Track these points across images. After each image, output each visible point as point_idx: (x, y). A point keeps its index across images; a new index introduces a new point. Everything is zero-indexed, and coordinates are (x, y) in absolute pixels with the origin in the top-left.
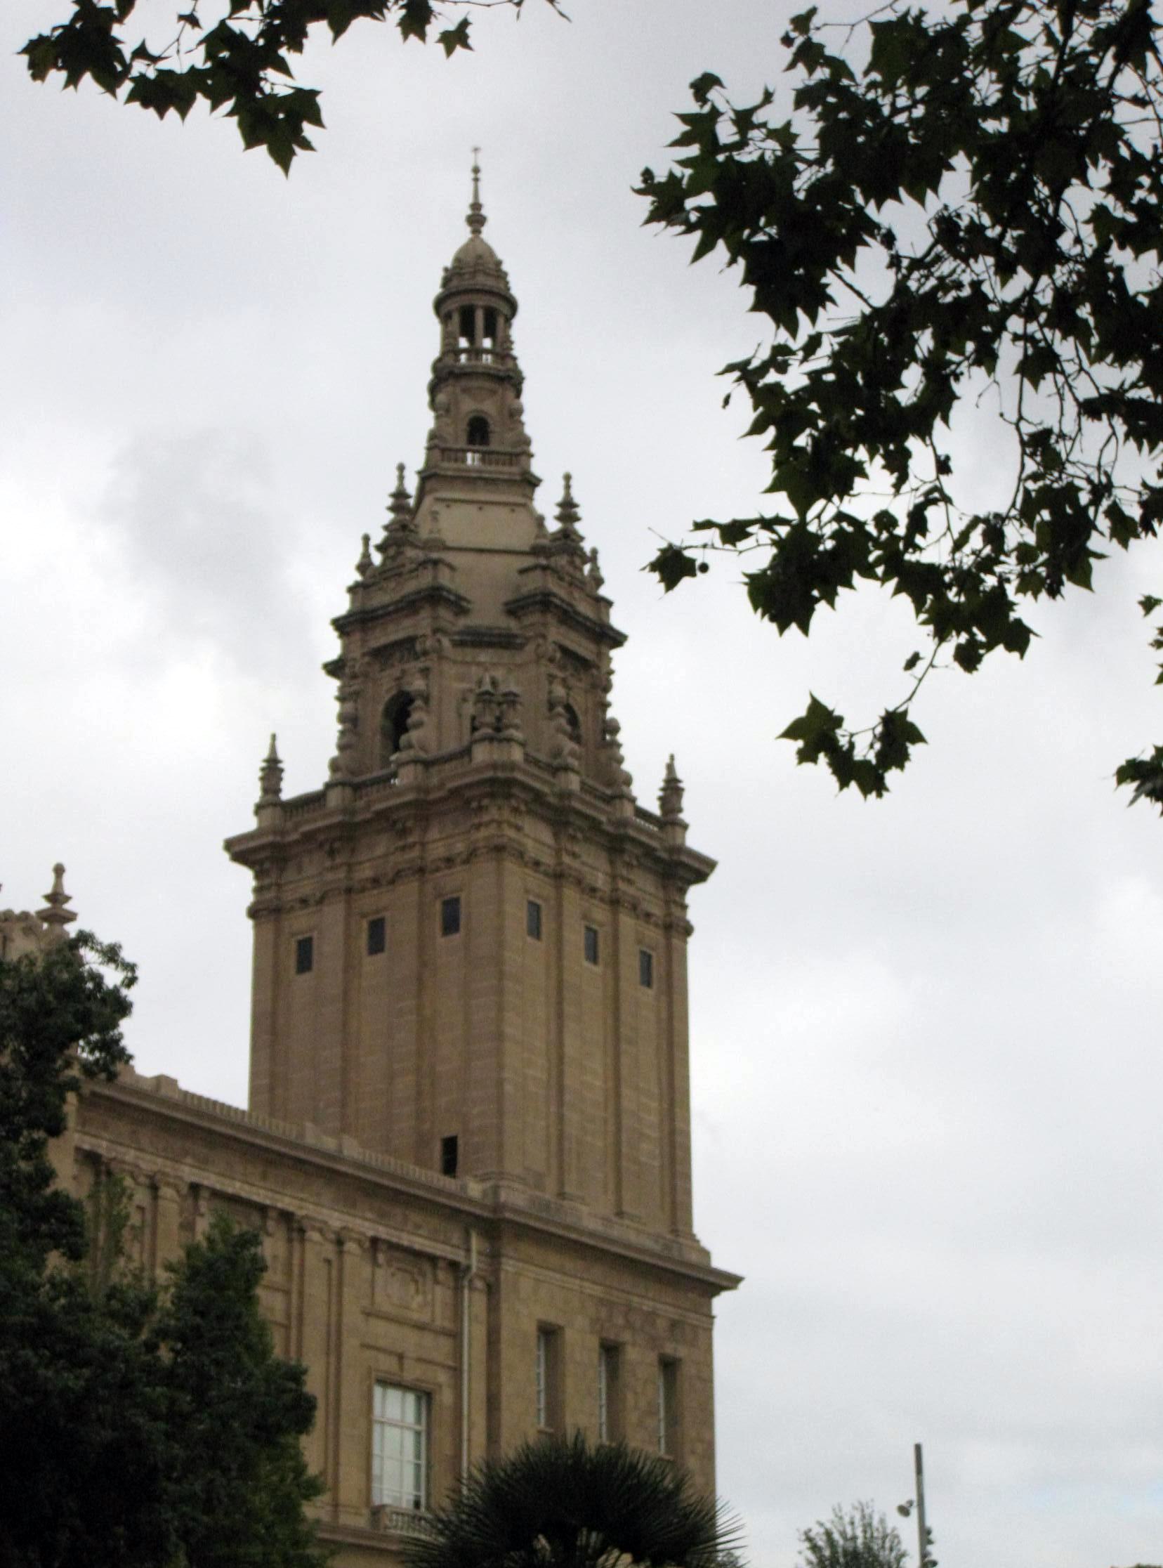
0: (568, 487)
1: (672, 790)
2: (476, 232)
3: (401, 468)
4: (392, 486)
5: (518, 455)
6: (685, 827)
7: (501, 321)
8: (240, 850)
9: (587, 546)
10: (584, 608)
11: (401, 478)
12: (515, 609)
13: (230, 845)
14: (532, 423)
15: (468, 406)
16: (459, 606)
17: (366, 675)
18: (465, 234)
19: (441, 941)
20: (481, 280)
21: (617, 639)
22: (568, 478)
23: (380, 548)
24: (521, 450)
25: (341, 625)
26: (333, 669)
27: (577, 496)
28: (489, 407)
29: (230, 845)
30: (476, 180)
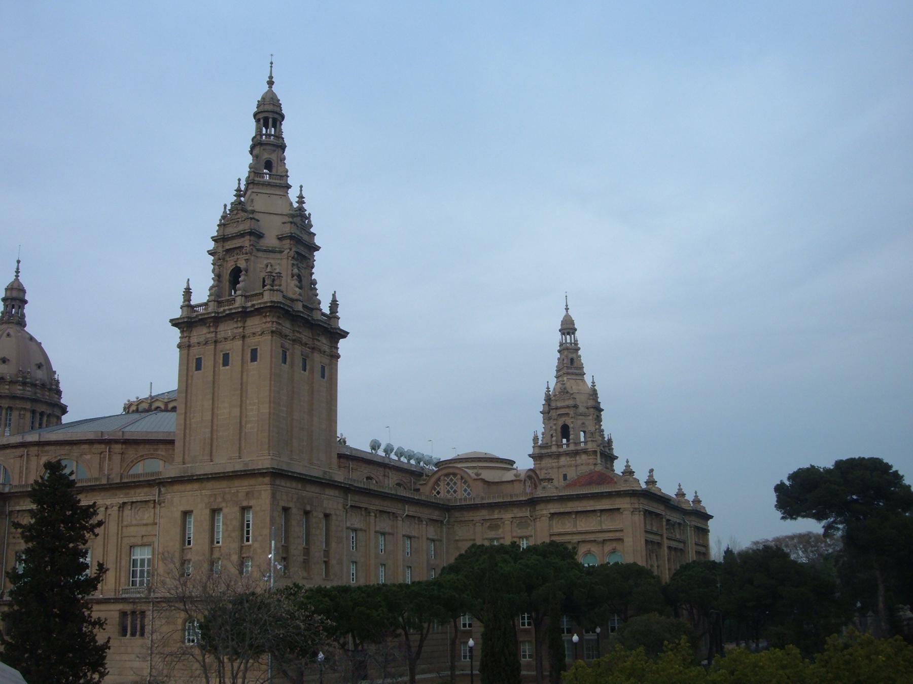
0: (301, 190)
1: (334, 305)
2: (270, 87)
3: (239, 180)
4: (236, 187)
7: (278, 123)
8: (175, 323)
9: (307, 213)
10: (305, 237)
11: (239, 184)
13: (171, 321)
15: (266, 156)
16: (260, 236)
17: (224, 259)
21: (317, 248)
22: (301, 187)
25: (215, 239)
26: (211, 253)
28: (273, 157)
29: (171, 321)
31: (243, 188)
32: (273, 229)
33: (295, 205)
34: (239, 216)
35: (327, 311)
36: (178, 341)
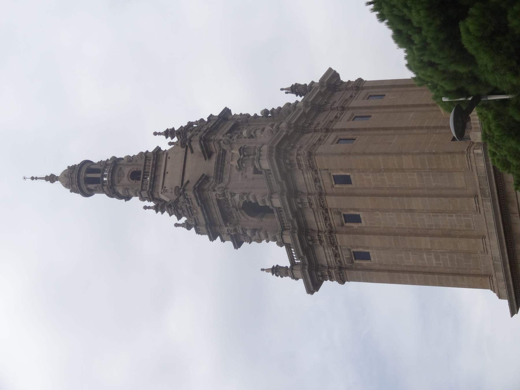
0: (160, 134)
1: (295, 89)
3: (145, 208)
5: (146, 157)
6: (313, 82)
7: (93, 167)
8: (313, 286)
11: (149, 208)
12: (207, 154)
14: (134, 152)
15: (126, 180)
16: (205, 178)
18: (58, 183)
19: (353, 185)
20: (74, 175)
22: (155, 134)
23: (179, 218)
24: (145, 155)
27: (162, 130)
28: (127, 171)
30: (36, 178)
31: (152, 204)
32: (198, 166)
33: (175, 140)
34: (184, 208)
35: (300, 99)
36: (335, 283)
